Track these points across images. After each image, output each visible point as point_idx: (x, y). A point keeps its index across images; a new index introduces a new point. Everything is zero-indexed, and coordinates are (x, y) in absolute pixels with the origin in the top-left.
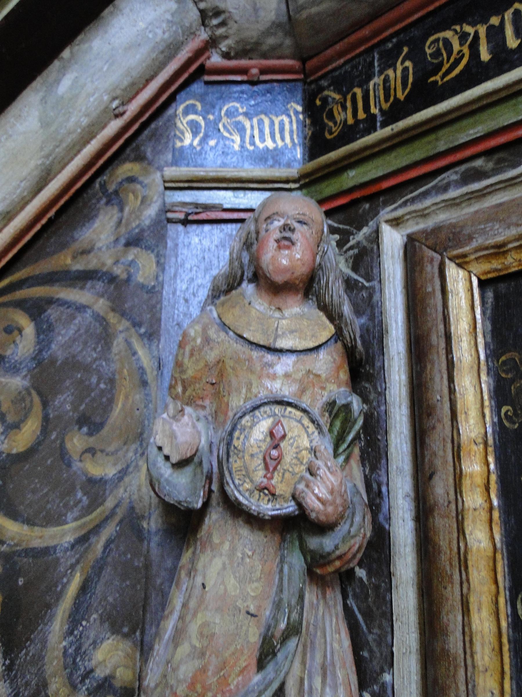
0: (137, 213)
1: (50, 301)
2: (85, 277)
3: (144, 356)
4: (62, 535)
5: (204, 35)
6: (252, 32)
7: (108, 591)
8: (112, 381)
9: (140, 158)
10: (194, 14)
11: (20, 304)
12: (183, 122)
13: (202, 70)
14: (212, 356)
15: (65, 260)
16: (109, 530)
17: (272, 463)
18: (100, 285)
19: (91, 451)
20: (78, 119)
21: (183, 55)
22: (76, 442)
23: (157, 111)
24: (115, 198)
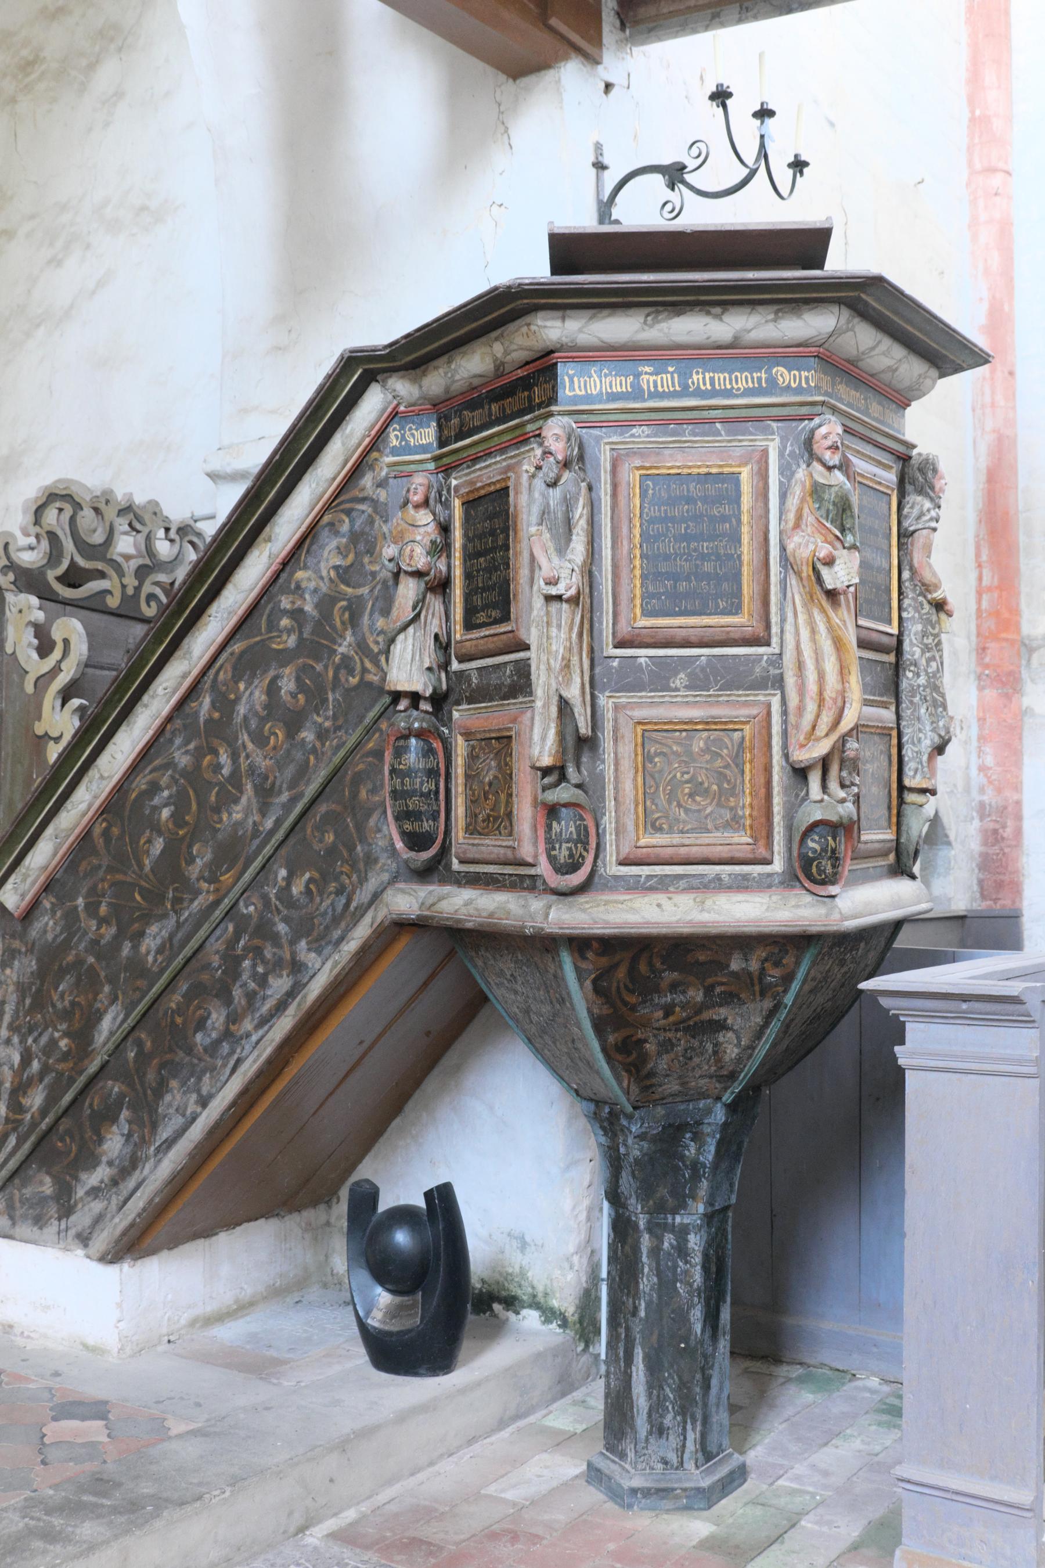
0: (379, 474)
1: (353, 509)
2: (364, 500)
3: (385, 529)
4: (365, 591)
5: (395, 402)
6: (413, 400)
7: (380, 604)
8: (375, 538)
9: (379, 450)
10: (390, 397)
11: (342, 511)
12: (392, 436)
13: (397, 413)
14: (399, 529)
15: (356, 493)
16: (379, 587)
17: (411, 557)
18: (368, 502)
19: (370, 562)
20: (354, 441)
21: (389, 410)
22: (366, 560)
23: (383, 431)
24: (372, 467)
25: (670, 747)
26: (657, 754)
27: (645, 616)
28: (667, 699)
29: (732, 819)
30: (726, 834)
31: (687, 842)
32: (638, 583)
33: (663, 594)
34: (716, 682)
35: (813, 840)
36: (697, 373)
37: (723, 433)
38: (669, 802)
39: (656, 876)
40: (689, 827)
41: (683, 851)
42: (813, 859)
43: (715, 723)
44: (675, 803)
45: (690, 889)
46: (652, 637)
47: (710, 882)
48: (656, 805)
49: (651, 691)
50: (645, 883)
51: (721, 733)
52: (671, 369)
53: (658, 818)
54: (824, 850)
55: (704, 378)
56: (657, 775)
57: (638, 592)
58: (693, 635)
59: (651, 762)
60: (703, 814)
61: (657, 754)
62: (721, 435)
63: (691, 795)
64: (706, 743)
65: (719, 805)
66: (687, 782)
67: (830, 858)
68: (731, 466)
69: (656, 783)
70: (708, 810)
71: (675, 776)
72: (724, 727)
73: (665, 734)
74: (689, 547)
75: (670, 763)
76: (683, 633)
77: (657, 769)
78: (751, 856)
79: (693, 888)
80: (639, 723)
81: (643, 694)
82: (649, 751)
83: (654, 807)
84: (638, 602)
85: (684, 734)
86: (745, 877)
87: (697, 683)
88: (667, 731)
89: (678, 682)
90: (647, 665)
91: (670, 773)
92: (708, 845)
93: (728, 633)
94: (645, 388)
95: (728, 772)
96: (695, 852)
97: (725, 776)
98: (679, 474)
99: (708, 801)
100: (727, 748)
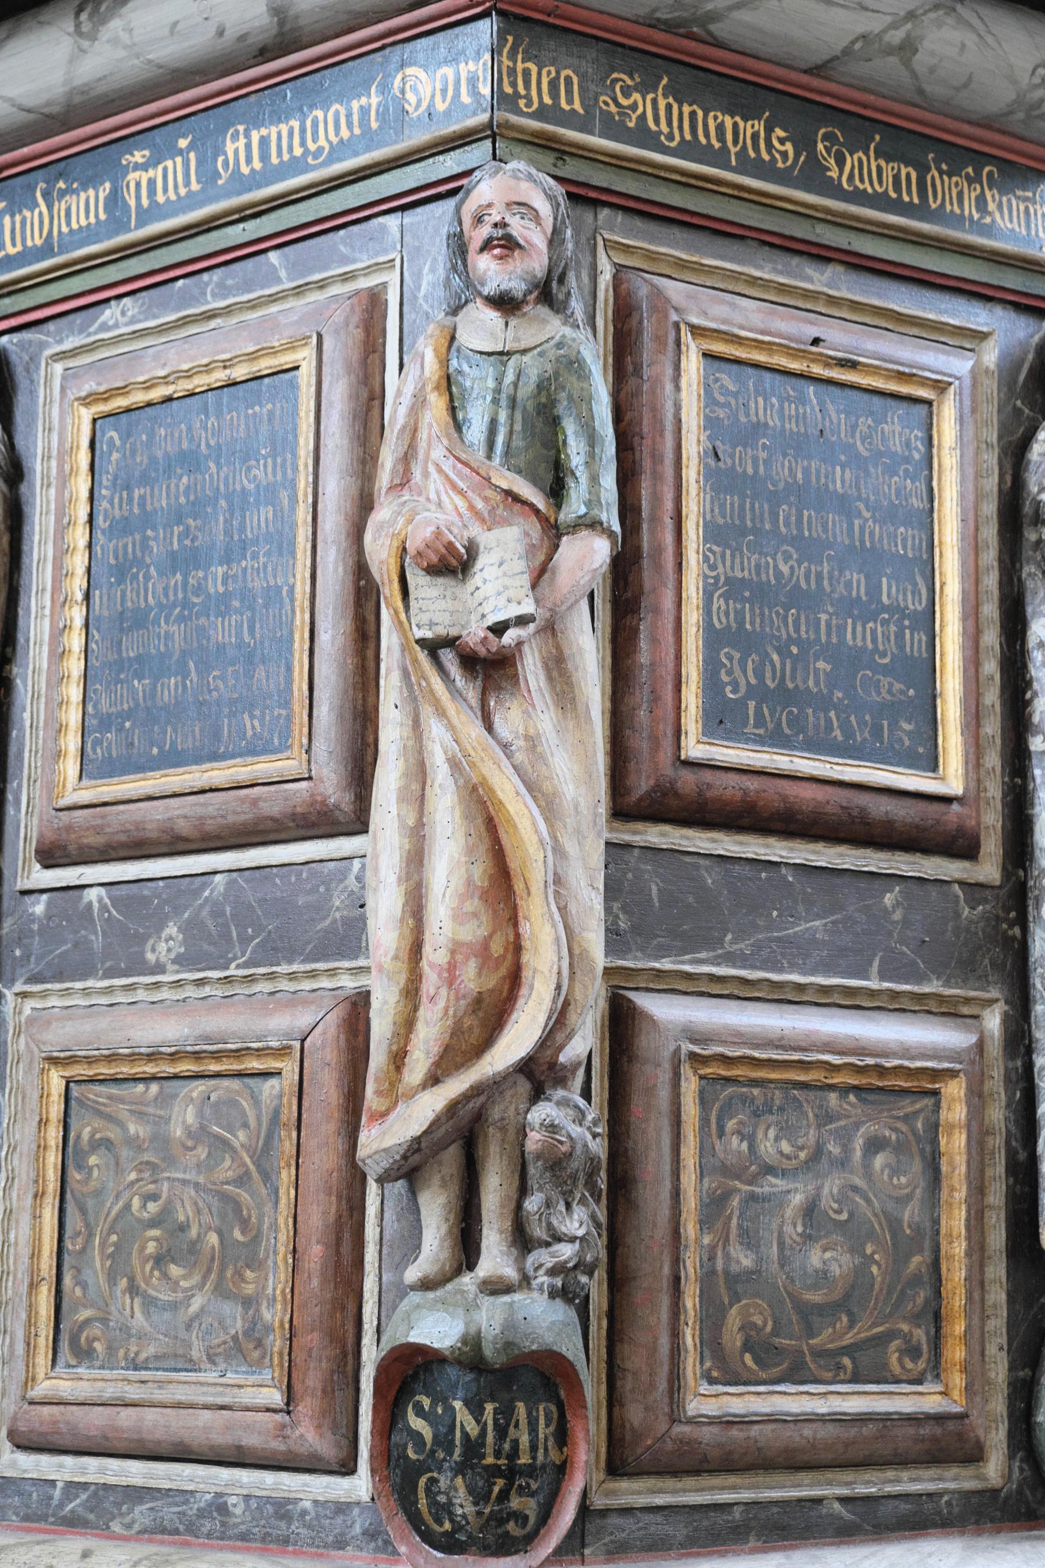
25: (122, 1125)
26: (96, 1145)
27: (91, 777)
28: (141, 995)
29: (246, 1333)
30: (231, 1378)
31: (134, 1393)
32: (74, 692)
33: (129, 715)
34: (244, 940)
35: (420, 1412)
36: (235, 137)
37: (283, 274)
38: (112, 1280)
39: (85, 1485)
40: (151, 1350)
41: (126, 1417)
42: (420, 1468)
43: (216, 1056)
44: (124, 1283)
45: (158, 1531)
46: (98, 830)
47: (201, 1514)
48: (85, 1287)
49: (109, 974)
50: (61, 1505)
51: (235, 1084)
52: (183, 143)
53: (87, 1322)
54: (444, 1441)
55: (248, 146)
56: (90, 1203)
57: (73, 717)
58: (180, 814)
59: (79, 1167)
60: (183, 1316)
61: (96, 1145)
62: (279, 280)
63: (159, 1261)
64: (200, 1114)
65: (221, 1291)
66: (154, 1223)
67: (460, 1469)
68: (274, 352)
69: (87, 1225)
70: (197, 1303)
71: (128, 1206)
72: (236, 1067)
73: (114, 1090)
74: (185, 583)
75: (118, 1168)
76: (156, 813)
77: (93, 1184)
78: (277, 1445)
79: (163, 1531)
80: (53, 1061)
81: (90, 983)
82: (78, 1137)
83: (78, 1292)
84: (72, 742)
85: (154, 1088)
86: (282, 1508)
87: (202, 953)
88: (115, 1080)
89: (162, 947)
90: (103, 908)
91: (117, 1197)
92: (179, 1406)
93: (255, 802)
94: (132, 203)
95: (245, 1196)
96: (155, 1424)
97: (237, 1206)
98: (169, 399)
99: (196, 1279)
100: (245, 1125)
